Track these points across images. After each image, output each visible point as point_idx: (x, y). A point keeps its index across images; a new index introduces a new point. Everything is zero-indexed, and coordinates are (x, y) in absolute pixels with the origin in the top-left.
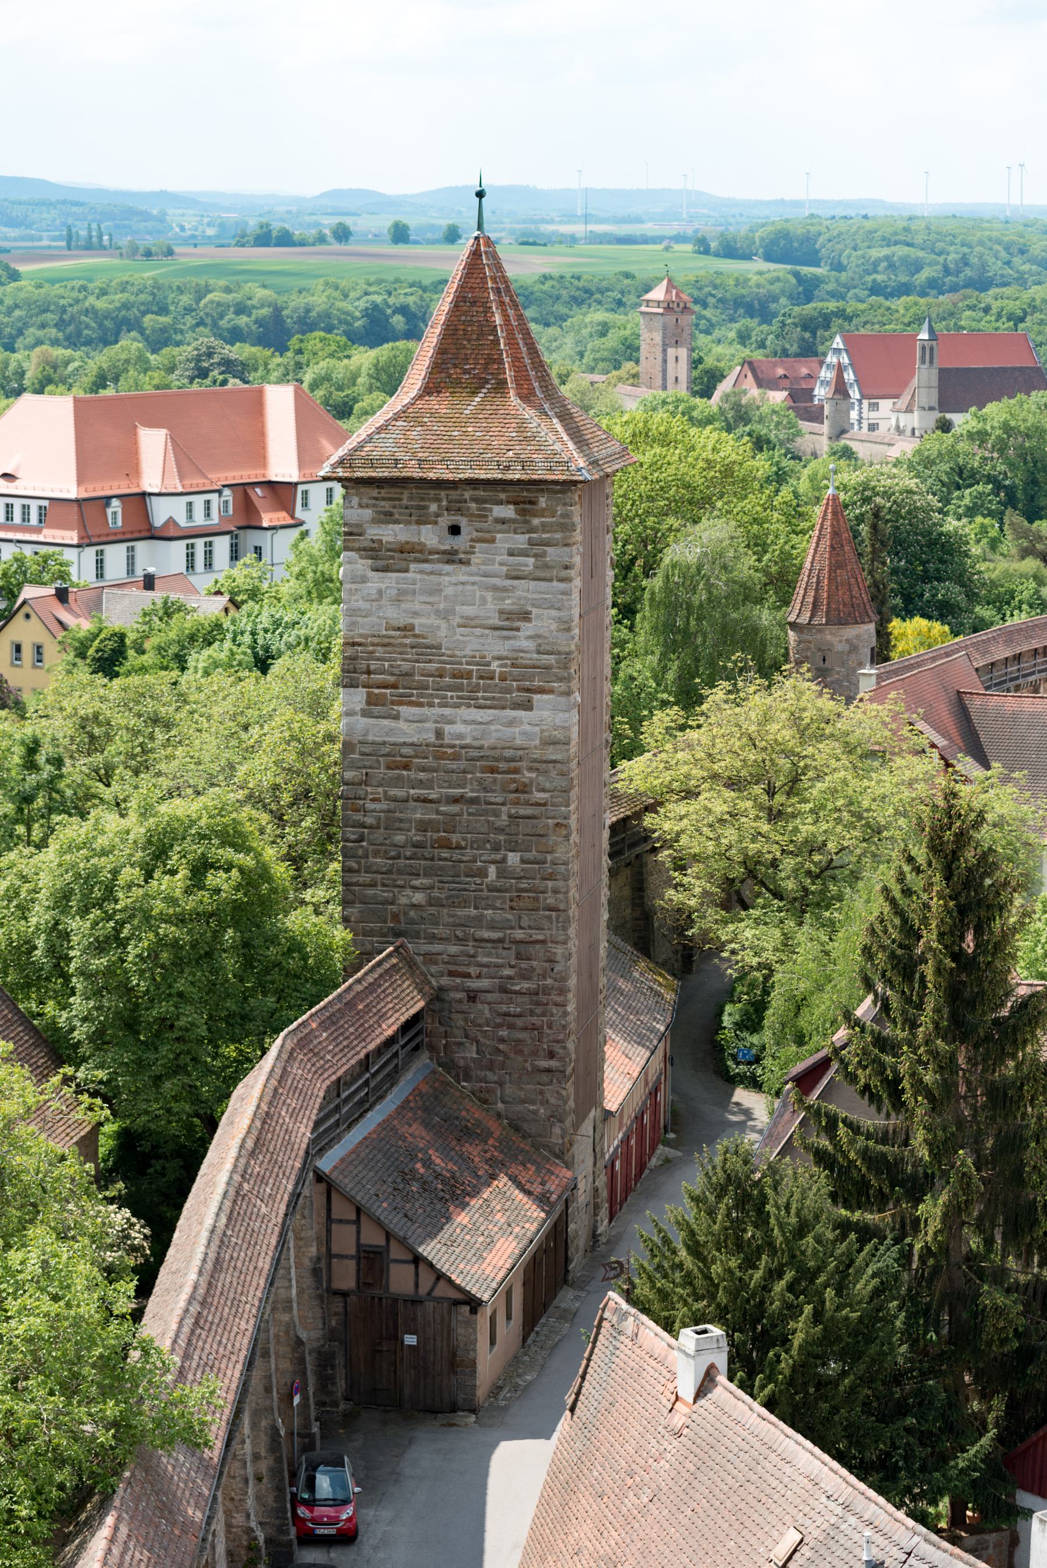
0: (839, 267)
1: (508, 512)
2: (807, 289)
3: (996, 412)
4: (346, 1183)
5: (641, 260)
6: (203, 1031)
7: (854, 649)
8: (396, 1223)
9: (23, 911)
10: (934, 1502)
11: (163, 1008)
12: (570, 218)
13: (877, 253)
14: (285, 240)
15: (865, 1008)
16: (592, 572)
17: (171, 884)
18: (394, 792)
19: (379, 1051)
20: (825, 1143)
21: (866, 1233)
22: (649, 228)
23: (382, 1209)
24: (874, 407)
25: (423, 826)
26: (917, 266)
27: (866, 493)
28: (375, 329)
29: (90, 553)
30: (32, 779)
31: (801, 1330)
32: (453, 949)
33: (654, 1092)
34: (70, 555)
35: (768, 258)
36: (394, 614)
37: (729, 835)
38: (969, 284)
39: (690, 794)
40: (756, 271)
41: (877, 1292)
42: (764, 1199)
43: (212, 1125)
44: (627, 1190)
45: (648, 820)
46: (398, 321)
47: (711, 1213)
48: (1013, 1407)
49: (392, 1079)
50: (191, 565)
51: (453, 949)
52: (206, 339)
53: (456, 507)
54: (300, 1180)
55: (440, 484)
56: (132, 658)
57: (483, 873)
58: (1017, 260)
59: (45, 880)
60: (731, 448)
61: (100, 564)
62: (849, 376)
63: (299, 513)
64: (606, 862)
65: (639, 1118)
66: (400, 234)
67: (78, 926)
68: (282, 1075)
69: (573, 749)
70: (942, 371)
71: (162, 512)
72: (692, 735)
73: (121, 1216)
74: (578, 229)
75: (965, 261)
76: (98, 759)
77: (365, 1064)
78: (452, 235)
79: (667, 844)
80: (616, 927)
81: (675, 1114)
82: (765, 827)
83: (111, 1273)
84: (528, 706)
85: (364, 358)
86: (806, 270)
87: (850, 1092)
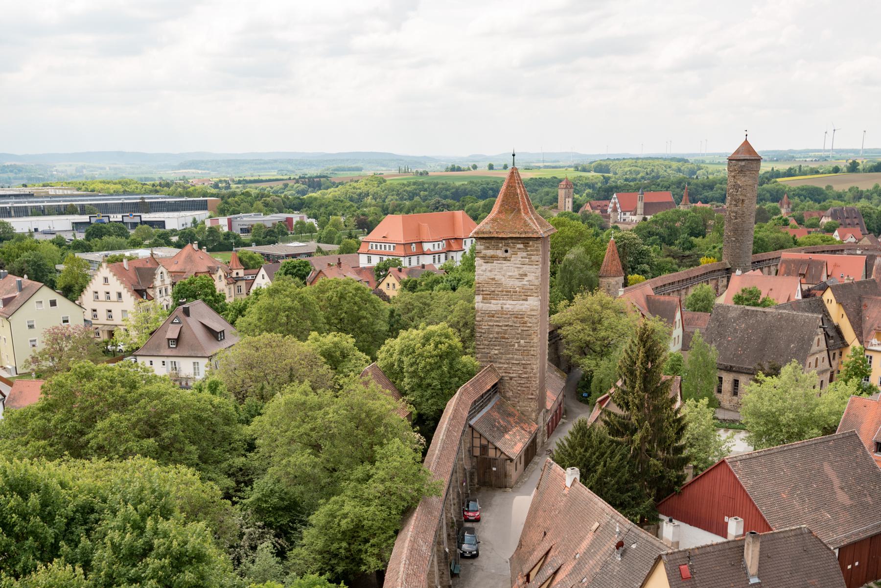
0: (615, 174)
1: (521, 246)
2: (607, 180)
3: (660, 214)
4: (477, 428)
5: (560, 174)
6: (439, 387)
7: (617, 283)
8: (490, 438)
9: (391, 355)
10: (636, 516)
11: (429, 381)
12: (538, 161)
13: (627, 169)
14: (459, 169)
15: (619, 383)
16: (544, 263)
17: (430, 347)
18: (491, 324)
19: (486, 393)
20: (607, 419)
21: (618, 443)
22: (561, 164)
23: (487, 435)
24: (625, 214)
25: (498, 333)
26: (638, 173)
27: (622, 238)
28: (484, 195)
29: (407, 259)
30: (393, 320)
31: (600, 468)
32: (506, 366)
33: (560, 405)
34: (402, 259)
35: (595, 171)
36: (489, 274)
37: (581, 335)
38: (653, 177)
39: (570, 324)
40: (591, 174)
41: (621, 460)
42: (590, 434)
43: (441, 411)
44: (553, 431)
45: (559, 331)
46: (491, 192)
47: (576, 438)
48: (659, 491)
49: (489, 400)
50: (434, 261)
51: (506, 366)
52: (437, 198)
53: (507, 245)
54: (465, 427)
55: (502, 239)
56: (419, 288)
57: (514, 345)
58: (668, 170)
59: (397, 347)
60: (583, 227)
61: (410, 261)
62: (618, 206)
63: (464, 247)
64: (548, 342)
65: (556, 411)
66: (491, 167)
67: (404, 359)
68: (460, 399)
69: (539, 312)
70: (645, 204)
71: (427, 247)
72: (571, 308)
73: (418, 436)
74: (541, 165)
75: (653, 171)
76: (410, 315)
77: (482, 396)
78: (505, 167)
79: (564, 338)
80: (550, 360)
81: (566, 411)
82: (591, 333)
83: (415, 450)
84: (526, 300)
85: (481, 203)
86: (606, 175)
87: (614, 405)
